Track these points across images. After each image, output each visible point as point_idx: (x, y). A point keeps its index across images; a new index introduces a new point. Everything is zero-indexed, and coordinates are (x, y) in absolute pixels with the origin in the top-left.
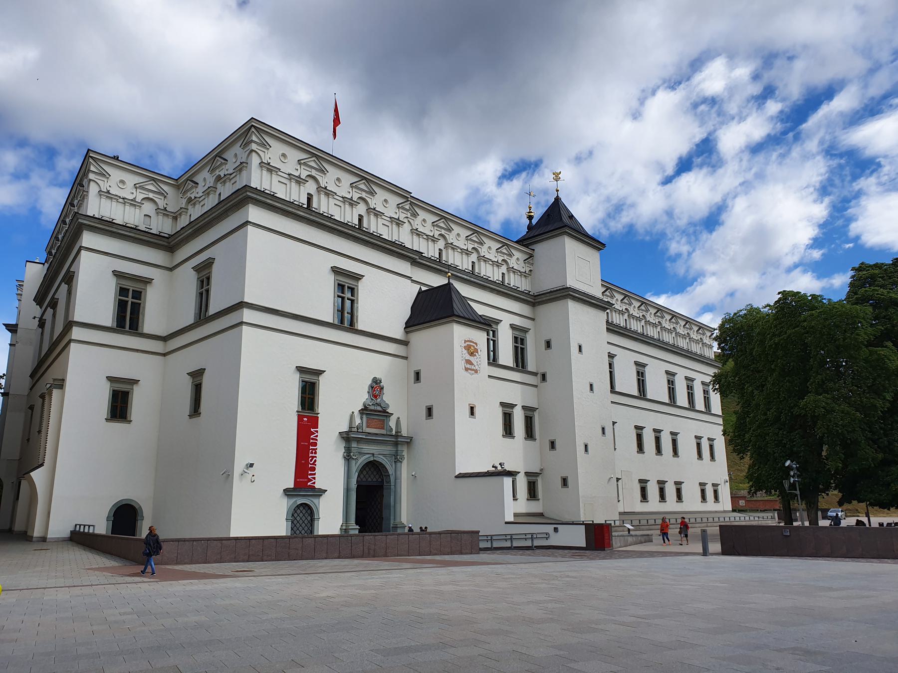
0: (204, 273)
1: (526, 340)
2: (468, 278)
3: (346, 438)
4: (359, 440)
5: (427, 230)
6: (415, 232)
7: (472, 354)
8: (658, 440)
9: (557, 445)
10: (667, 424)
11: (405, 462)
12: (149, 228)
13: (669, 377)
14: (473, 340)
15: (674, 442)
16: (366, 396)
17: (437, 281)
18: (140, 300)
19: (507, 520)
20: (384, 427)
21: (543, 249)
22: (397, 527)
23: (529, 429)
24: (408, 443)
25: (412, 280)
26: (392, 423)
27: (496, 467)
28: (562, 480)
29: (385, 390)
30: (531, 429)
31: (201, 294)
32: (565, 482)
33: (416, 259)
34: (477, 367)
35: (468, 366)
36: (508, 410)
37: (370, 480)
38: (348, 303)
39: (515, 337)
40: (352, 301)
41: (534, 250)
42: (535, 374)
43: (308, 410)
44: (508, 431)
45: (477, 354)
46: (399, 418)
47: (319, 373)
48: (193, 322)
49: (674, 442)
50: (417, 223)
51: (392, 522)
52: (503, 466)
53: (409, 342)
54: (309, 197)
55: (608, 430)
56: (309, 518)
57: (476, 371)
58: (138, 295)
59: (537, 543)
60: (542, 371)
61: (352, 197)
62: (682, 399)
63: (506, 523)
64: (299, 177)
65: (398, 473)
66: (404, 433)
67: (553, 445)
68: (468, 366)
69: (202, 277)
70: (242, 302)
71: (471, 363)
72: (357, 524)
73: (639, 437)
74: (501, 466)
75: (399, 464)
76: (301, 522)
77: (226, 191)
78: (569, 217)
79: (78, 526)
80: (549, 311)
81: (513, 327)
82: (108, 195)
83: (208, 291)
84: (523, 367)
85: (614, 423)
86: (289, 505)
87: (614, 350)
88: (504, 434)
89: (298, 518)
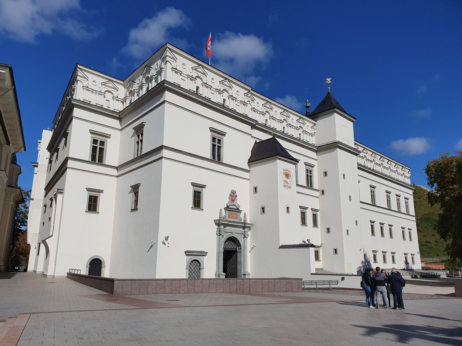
0: (139, 130)
2: (282, 136)
4: (225, 225)
5: (261, 109)
6: (254, 109)
10: (387, 220)
12: (108, 107)
14: (288, 170)
16: (228, 200)
17: (265, 137)
18: (103, 146)
19: (312, 272)
20: (237, 218)
22: (245, 275)
23: (315, 222)
25: (252, 136)
26: (242, 216)
27: (305, 242)
30: (316, 221)
33: (254, 125)
34: (290, 185)
35: (286, 184)
36: (303, 210)
37: (230, 247)
39: (307, 170)
40: (219, 147)
43: (197, 207)
44: (304, 222)
46: (245, 213)
47: (203, 187)
48: (133, 158)
50: (254, 105)
51: (242, 271)
52: (309, 242)
54: (197, 88)
56: (198, 268)
57: (290, 187)
58: (102, 143)
59: (332, 286)
60: (322, 189)
61: (220, 89)
62: (394, 206)
63: (312, 274)
64: (192, 76)
65: (245, 244)
66: (248, 222)
68: (286, 184)
69: (138, 133)
70: (162, 145)
71: (287, 183)
72: (224, 272)
74: (308, 241)
75: (245, 239)
76: (194, 270)
77: (153, 84)
79: (71, 270)
81: (306, 164)
82: (87, 88)
84: (311, 187)
86: (188, 261)
88: (302, 224)
89: (192, 268)
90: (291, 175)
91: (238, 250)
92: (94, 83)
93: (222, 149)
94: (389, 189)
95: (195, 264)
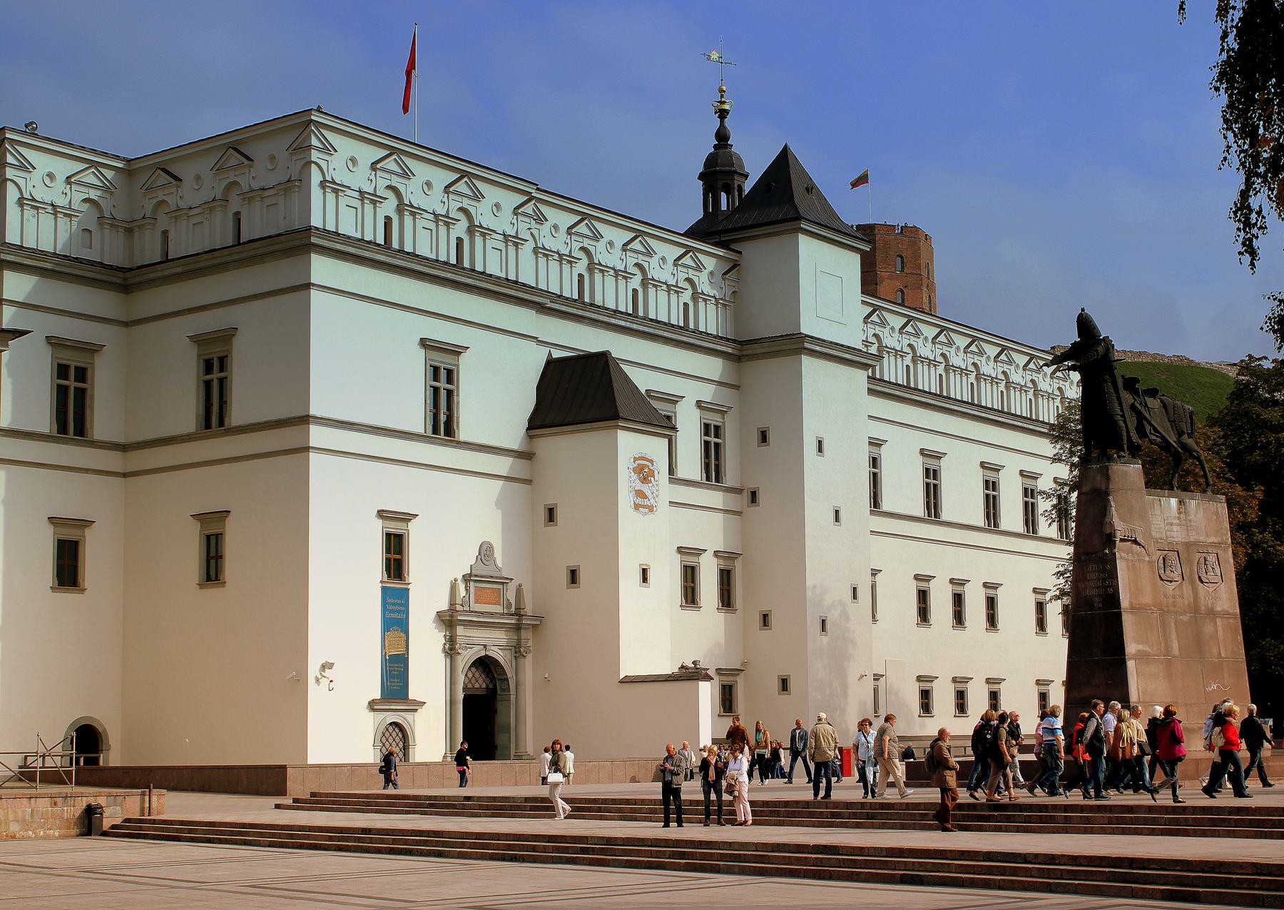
1: (724, 429)
3: (448, 620)
4: (467, 624)
7: (645, 480)
8: (958, 600)
9: (773, 620)
11: (529, 657)
13: (989, 473)
15: (991, 603)
21: (757, 252)
23: (726, 593)
24: (534, 626)
28: (780, 681)
31: (208, 385)
32: (784, 684)
34: (652, 501)
35: (640, 501)
38: (443, 394)
41: (740, 253)
42: (737, 491)
44: (690, 596)
45: (652, 479)
47: (406, 518)
49: (991, 603)
53: (535, 454)
55: (865, 594)
57: (651, 509)
58: (82, 374)
60: (751, 485)
62: (1012, 516)
66: (529, 609)
67: (765, 620)
68: (640, 501)
73: (923, 596)
75: (521, 660)
78: (807, 189)
80: (766, 371)
83: (222, 381)
85: (875, 573)
87: (879, 431)
90: (656, 472)
91: (499, 692)
92: (48, 181)
94: (993, 457)
95: (394, 734)
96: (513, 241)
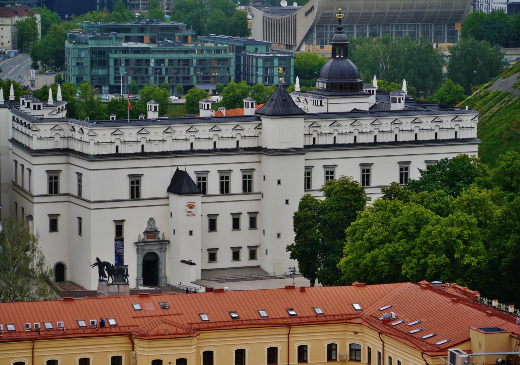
26: (160, 236)
29: (156, 222)
35: (189, 214)
57: (194, 215)
90: (196, 206)
93: (140, 188)
96: (163, 140)
